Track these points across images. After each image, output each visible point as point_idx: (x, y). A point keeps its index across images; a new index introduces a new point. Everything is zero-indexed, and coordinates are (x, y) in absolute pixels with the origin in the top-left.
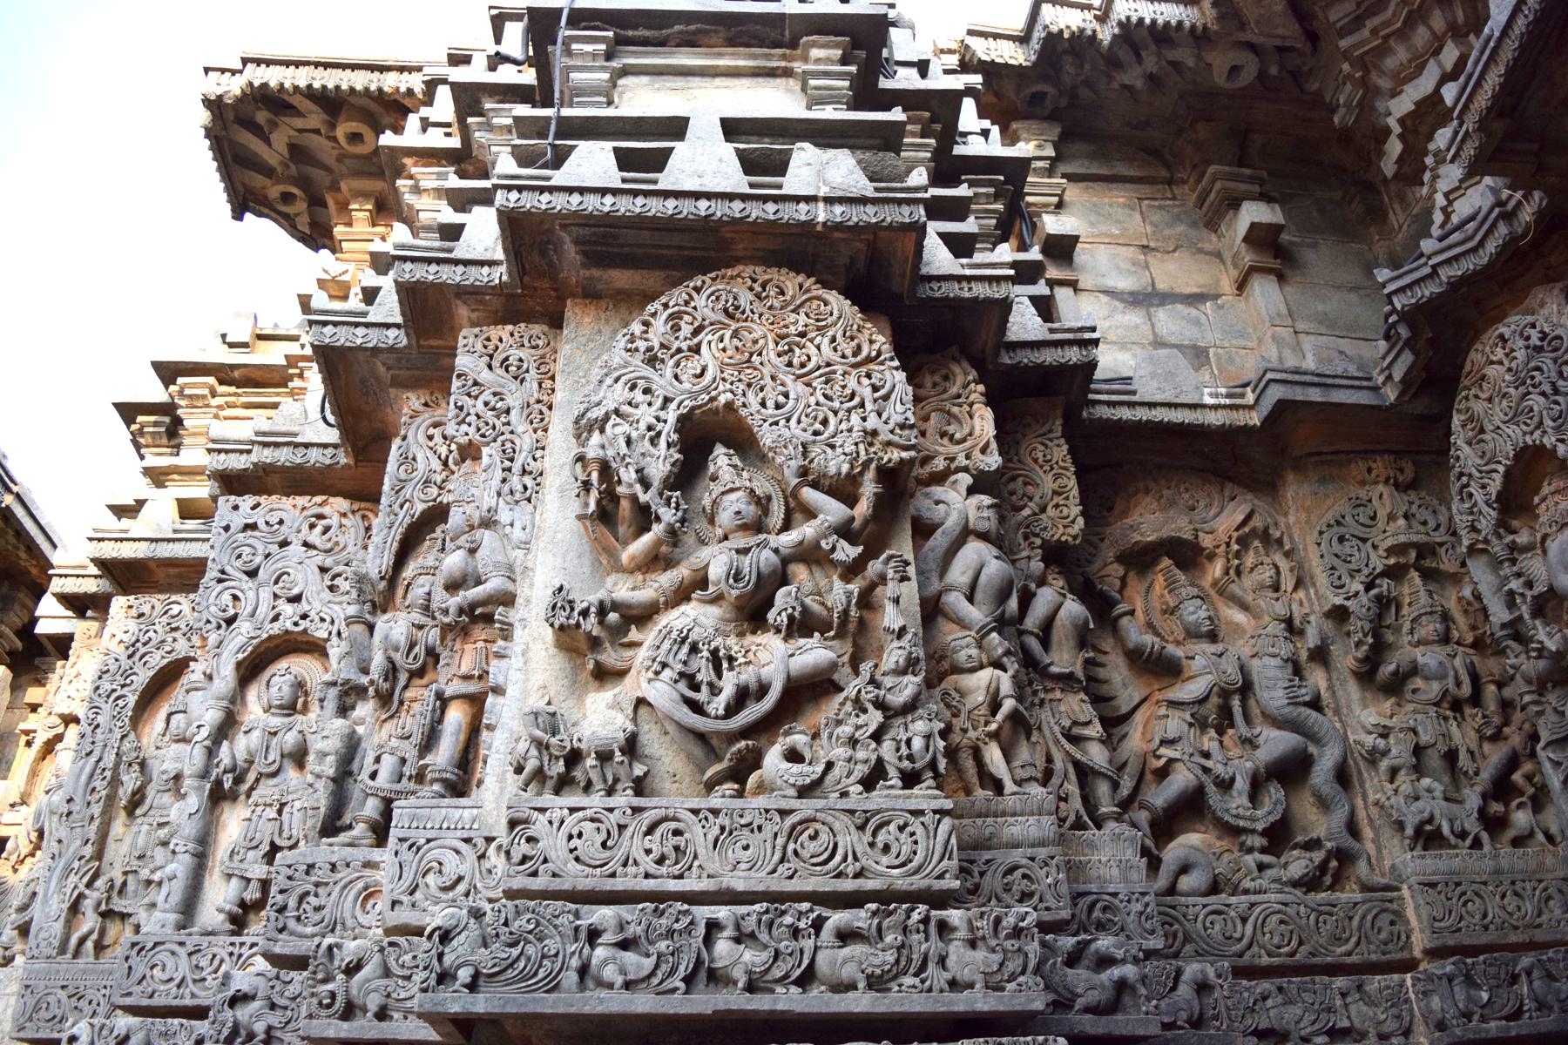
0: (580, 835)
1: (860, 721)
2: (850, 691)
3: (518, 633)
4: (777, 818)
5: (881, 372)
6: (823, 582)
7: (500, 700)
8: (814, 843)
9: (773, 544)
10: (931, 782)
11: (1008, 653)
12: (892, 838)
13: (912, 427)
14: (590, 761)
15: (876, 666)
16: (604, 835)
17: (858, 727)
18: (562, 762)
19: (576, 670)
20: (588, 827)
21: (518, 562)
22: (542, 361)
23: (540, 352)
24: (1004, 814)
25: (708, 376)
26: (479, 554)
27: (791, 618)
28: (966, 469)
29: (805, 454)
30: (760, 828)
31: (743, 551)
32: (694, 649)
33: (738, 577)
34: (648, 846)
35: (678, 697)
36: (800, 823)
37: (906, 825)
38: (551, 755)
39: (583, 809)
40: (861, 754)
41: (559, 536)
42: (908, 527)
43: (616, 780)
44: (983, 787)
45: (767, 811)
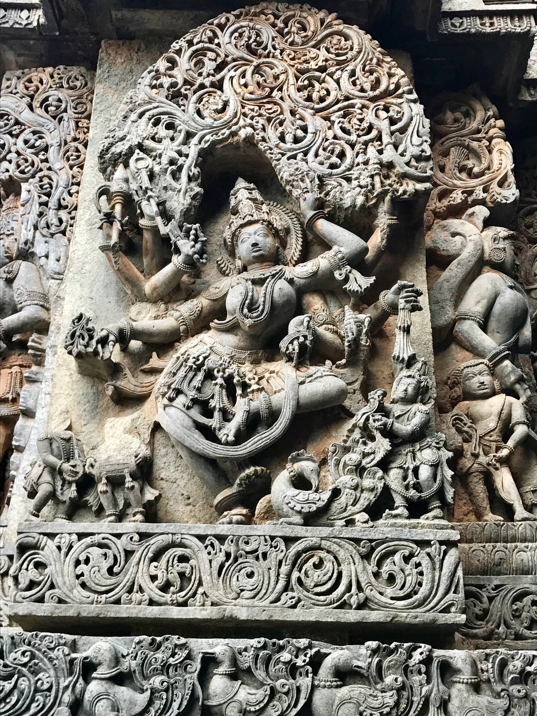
0: (87, 561)
1: (367, 449)
2: (359, 419)
3: (49, 359)
4: (282, 545)
5: (399, 105)
6: (336, 312)
7: (30, 422)
8: (319, 572)
9: (288, 275)
10: (437, 512)
11: (520, 380)
12: (396, 568)
13: (428, 159)
14: (101, 487)
15: (384, 394)
16: (111, 561)
17: (365, 455)
18: (74, 487)
19: (99, 394)
20: (96, 552)
21: (52, 292)
22: (79, 101)
23: (78, 93)
24: (514, 539)
25: (230, 111)
26: (15, 284)
27: (302, 346)
28: (483, 202)
29: (321, 186)
30: (265, 555)
31: (258, 282)
32: (209, 376)
33: (252, 306)
34: (153, 572)
35: (190, 423)
36: (305, 550)
37: (412, 555)
38: (64, 480)
39: (92, 534)
40: (367, 482)
41: (87, 267)
42: (423, 258)
43: (127, 505)
44: (493, 512)
45: (272, 538)
